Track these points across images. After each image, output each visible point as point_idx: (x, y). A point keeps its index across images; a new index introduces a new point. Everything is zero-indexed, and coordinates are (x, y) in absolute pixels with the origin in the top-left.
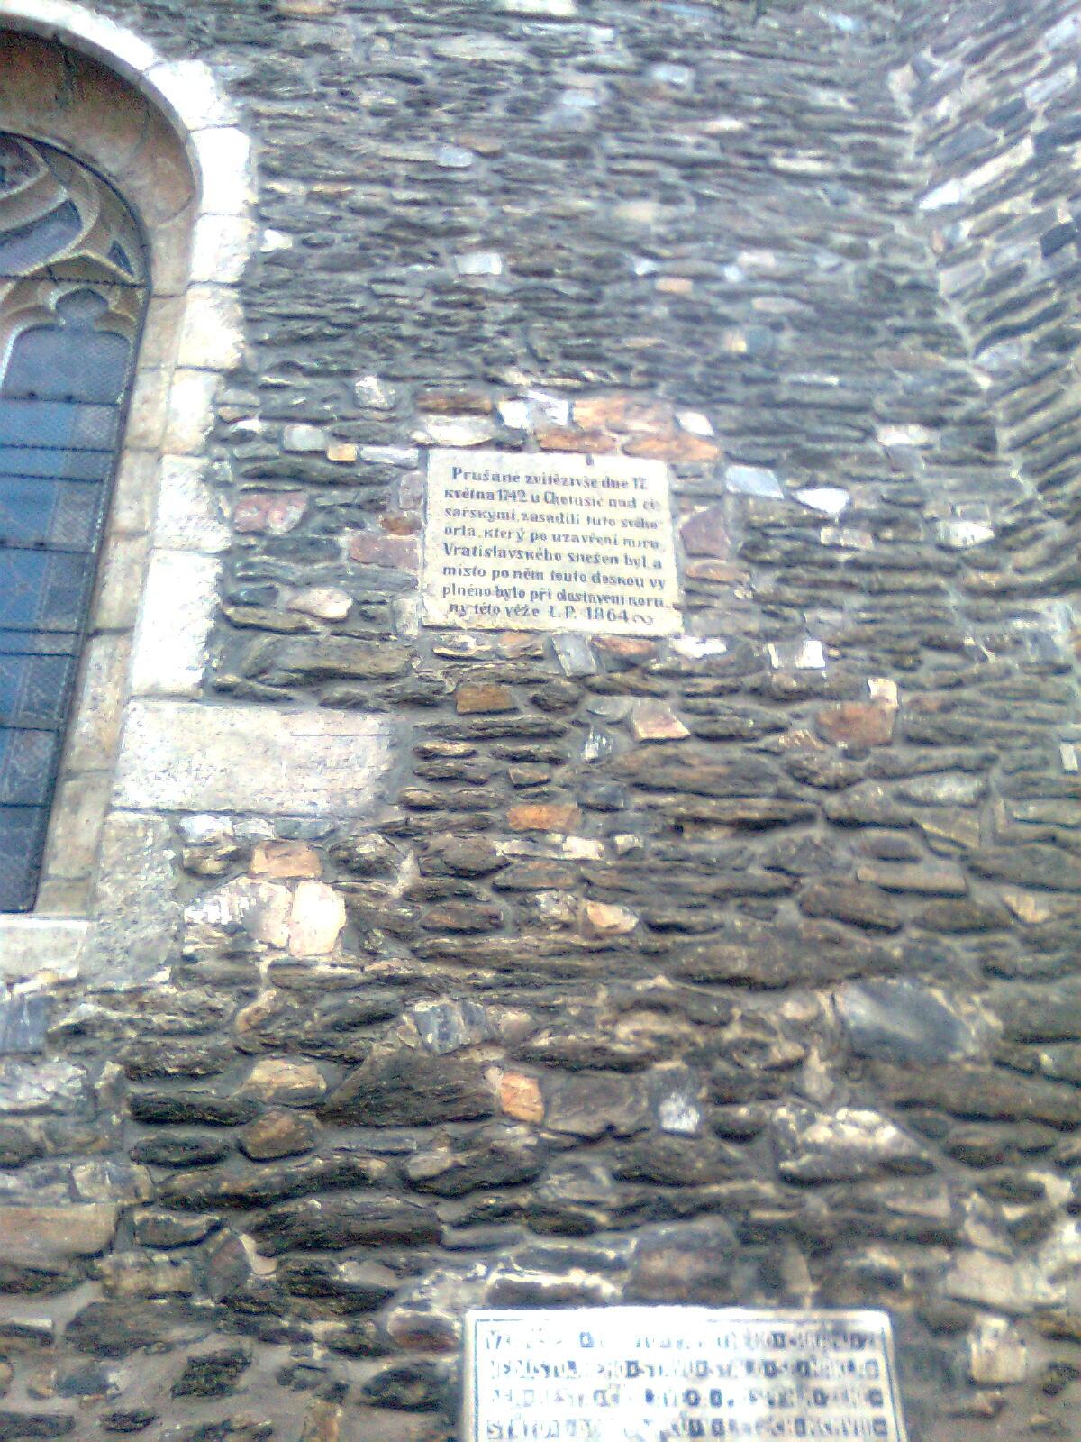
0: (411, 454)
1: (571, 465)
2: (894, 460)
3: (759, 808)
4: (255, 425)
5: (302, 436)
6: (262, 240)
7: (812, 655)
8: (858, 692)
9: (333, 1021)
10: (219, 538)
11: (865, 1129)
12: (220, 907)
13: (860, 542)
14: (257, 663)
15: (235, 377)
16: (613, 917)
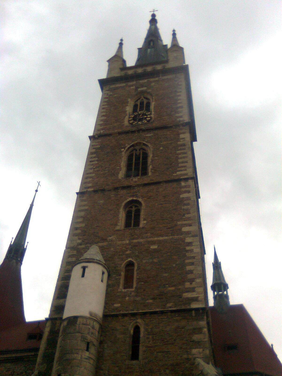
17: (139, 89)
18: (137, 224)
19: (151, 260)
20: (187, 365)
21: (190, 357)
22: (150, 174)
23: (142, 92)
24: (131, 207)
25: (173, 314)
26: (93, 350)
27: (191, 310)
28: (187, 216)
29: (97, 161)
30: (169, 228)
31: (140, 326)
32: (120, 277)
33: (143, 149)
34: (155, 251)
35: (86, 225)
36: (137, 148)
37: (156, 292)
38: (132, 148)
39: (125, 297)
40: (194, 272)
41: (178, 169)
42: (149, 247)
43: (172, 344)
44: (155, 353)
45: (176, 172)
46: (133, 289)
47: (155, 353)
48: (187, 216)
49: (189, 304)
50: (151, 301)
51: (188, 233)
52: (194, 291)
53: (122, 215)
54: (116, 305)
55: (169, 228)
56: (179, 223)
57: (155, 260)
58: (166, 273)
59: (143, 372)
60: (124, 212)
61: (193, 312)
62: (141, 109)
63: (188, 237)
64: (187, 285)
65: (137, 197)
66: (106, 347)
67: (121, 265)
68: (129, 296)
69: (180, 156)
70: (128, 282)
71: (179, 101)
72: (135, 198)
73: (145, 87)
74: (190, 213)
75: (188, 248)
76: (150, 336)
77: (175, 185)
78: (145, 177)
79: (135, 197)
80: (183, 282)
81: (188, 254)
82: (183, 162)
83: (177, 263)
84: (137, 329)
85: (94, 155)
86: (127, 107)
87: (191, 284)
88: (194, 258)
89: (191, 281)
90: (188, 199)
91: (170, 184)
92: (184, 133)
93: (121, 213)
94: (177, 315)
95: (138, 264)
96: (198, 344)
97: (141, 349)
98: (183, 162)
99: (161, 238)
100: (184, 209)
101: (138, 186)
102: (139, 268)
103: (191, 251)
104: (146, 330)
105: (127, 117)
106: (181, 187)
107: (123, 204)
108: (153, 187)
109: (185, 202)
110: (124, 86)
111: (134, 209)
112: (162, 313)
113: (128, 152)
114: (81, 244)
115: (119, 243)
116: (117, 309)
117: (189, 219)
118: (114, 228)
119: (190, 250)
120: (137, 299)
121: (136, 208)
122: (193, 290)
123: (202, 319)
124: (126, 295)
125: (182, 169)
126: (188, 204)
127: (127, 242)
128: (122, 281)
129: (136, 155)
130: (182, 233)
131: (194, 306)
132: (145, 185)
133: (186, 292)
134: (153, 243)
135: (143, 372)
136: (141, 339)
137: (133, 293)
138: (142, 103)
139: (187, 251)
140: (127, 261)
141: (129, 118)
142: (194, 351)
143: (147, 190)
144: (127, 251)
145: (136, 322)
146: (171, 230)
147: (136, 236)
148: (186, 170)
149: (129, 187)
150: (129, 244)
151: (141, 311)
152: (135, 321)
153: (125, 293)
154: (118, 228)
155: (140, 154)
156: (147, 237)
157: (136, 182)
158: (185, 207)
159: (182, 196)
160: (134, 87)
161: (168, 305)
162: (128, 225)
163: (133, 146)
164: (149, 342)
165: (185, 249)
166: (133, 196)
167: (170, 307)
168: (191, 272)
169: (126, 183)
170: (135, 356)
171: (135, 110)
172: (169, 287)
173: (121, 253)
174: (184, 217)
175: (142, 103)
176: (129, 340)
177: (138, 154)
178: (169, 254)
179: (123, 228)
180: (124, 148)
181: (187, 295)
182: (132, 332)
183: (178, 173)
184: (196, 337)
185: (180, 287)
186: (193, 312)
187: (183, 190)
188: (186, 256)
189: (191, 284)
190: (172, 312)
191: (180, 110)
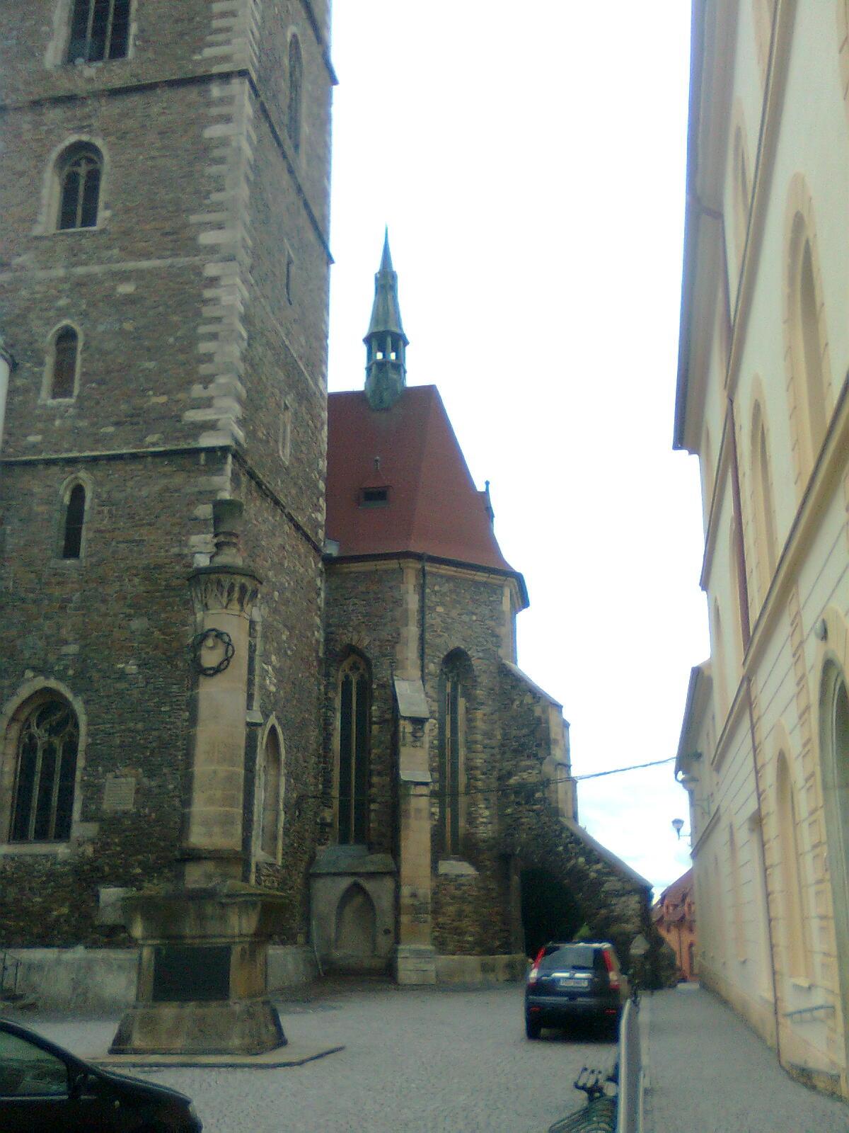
0: (104, 780)
1: (123, 780)
2: (165, 774)
3: (136, 832)
4: (86, 778)
5: (92, 779)
6: (87, 740)
7: (147, 811)
8: (151, 816)
9: (91, 862)
10: (82, 797)
11: (138, 871)
12: (81, 850)
13: (156, 791)
14: (86, 818)
15: (85, 769)
16: (118, 849)
18: (89, 219)
19: (117, 327)
20: (177, 567)
21: (186, 551)
22: (131, 52)
24: (77, 164)
25: (158, 460)
27: (198, 451)
28: (216, 197)
30: (167, 234)
31: (83, 484)
32: (42, 368)
34: (130, 300)
37: (123, 407)
39: (52, 419)
40: (217, 359)
41: (209, 38)
42: (114, 288)
43: (150, 524)
44: (114, 544)
45: (199, 50)
46: (72, 401)
47: (114, 544)
48: (216, 197)
49: (196, 437)
50: (111, 429)
51: (213, 249)
52: (210, 406)
53: (51, 190)
54: (32, 439)
55: (167, 234)
56: (193, 219)
57: (128, 326)
58: (151, 360)
59: (86, 582)
60: (57, 180)
61: (203, 456)
63: (211, 261)
64: (197, 390)
65: (90, 132)
66: (8, 532)
67: (44, 336)
68: (62, 417)
70: (62, 384)
72: (85, 138)
74: (220, 190)
75: (208, 294)
76: (106, 509)
77: (192, 94)
78: (115, 64)
79: (88, 132)
80: (187, 384)
81: (208, 311)
82: (224, 15)
83: (179, 334)
84: (78, 493)
87: (205, 388)
88: (218, 320)
89: (207, 380)
90: (224, 142)
91: (182, 92)
93: (48, 183)
94: (166, 463)
95: (86, 335)
97: (85, 535)
98: (224, 15)
99: (145, 264)
100: (210, 177)
101: (97, 95)
102: (87, 346)
103: (215, 301)
104: (98, 496)
106: (209, 104)
107: (54, 155)
108: (136, 100)
109: (216, 153)
111: (83, 170)
112: (134, 457)
115: (41, 275)
116: (34, 446)
117: (219, 207)
118: (30, 229)
119: (211, 300)
120: (81, 424)
121: (91, 167)
122: (207, 403)
123: (220, 471)
124: (55, 416)
125: (220, 37)
126: (221, 161)
128: (47, 379)
131: (207, 441)
132: (115, 93)
133: (193, 408)
134: (124, 277)
135: (86, 582)
136: (85, 514)
137: (71, 410)
139: (206, 302)
140: (59, 326)
142: (194, 539)
143: (118, 111)
144: (58, 298)
145: (76, 478)
146: (171, 241)
147: (84, 257)
148: (228, 42)
149: (69, 100)
150: (64, 280)
151: (87, 454)
152: (73, 476)
153: (52, 408)
154: (38, 230)
156: (110, 260)
157: (90, 80)
158: (214, 170)
161: (149, 439)
162: (67, 220)
164: (103, 520)
165: (200, 295)
166: (80, 129)
167: (154, 444)
168: (209, 358)
169: (64, 86)
170: (71, 549)
172: (155, 395)
173: (46, 305)
174: (207, 202)
176: (59, 517)
178: (161, 309)
179: (53, 229)
181: (193, 416)
182: (67, 500)
183: (208, 52)
186: (203, 456)
187: (214, 111)
188: (198, 313)
189: (205, 388)
190: (155, 455)
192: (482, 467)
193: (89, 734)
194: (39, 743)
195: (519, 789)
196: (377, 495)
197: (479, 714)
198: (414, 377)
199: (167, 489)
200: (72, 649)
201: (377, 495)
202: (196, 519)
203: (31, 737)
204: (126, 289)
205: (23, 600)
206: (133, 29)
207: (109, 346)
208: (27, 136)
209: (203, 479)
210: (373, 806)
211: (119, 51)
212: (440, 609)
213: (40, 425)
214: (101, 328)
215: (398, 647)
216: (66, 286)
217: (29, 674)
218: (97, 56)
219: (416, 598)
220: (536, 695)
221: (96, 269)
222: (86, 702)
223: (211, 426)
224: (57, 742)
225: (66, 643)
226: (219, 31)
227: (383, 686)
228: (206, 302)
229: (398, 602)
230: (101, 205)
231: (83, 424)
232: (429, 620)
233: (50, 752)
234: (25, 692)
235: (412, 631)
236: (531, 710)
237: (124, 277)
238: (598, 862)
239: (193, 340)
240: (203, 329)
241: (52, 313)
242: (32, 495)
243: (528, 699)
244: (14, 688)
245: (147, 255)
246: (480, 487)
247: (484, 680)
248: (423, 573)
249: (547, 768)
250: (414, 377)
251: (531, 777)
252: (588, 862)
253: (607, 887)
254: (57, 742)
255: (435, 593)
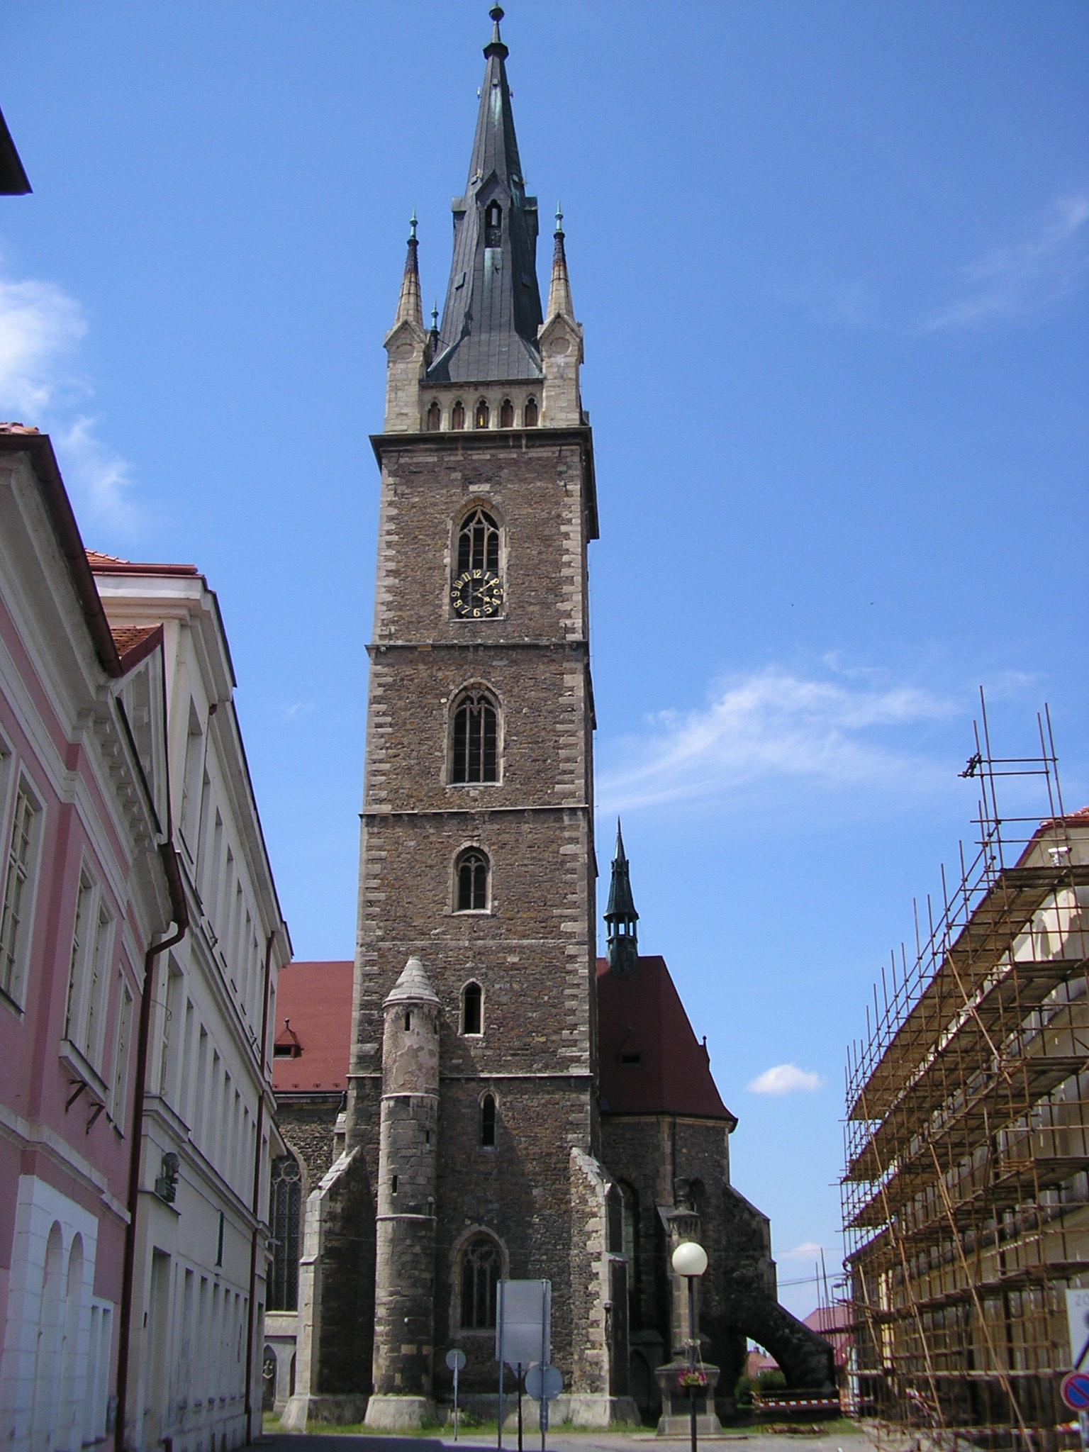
17: (472, 488)
18: (481, 904)
23: (479, 500)
24: (468, 860)
26: (433, 1139)
29: (391, 725)
33: (489, 702)
35: (389, 898)
36: (474, 694)
38: (464, 693)
41: (559, 777)
42: (505, 958)
46: (481, 1035)
51: (571, 935)
53: (452, 881)
56: (556, 912)
62: (478, 565)
69: (562, 740)
71: (565, 558)
72: (475, 844)
73: (488, 480)
75: (569, 967)
80: (558, 1031)
85: (383, 707)
86: (446, 552)
88: (578, 985)
89: (573, 1027)
90: (574, 857)
92: (573, 672)
96: (575, 1126)
98: (567, 760)
99: (526, 942)
103: (575, 972)
105: (447, 588)
106: (563, 829)
107: (454, 855)
110: (434, 464)
111: (473, 865)
113: (455, 705)
114: (382, 939)
117: (574, 905)
122: (574, 1043)
125: (566, 777)
126: (573, 871)
127: (467, 944)
129: (471, 712)
130: (561, 935)
134: (512, 950)
138: (479, 533)
139: (568, 972)
141: (453, 589)
142: (570, 1136)
154: (447, 910)
155: (479, 712)
159: (562, 850)
160: (458, 475)
163: (465, 688)
167: (540, 1071)
168: (572, 1012)
170: (488, 1139)
171: (462, 566)
175: (479, 533)
176: (479, 1117)
177: (475, 713)
180: (446, 695)
184: (572, 1117)
185: (554, 1038)
187: (567, 834)
191: (566, 589)
192: (700, 1028)
193: (511, 1262)
194: (475, 1266)
195: (742, 1279)
196: (634, 1059)
197: (711, 1227)
198: (643, 950)
199: (548, 1102)
200: (496, 1206)
201: (634, 1059)
202: (571, 1123)
203: (469, 1261)
204: (512, 959)
205: (460, 1172)
206: (502, 762)
207: (504, 999)
208: (433, 839)
209: (574, 1095)
210: (643, 1297)
211: (491, 775)
212: (684, 1151)
213: (460, 1052)
214: (497, 986)
215: (658, 1181)
216: (470, 953)
217: (468, 1222)
218: (474, 777)
219: (669, 1143)
220: (754, 1213)
221: (491, 943)
222: (507, 1242)
223: (577, 1060)
224: (487, 1266)
225: (491, 1202)
226: (565, 772)
227: (647, 1210)
228: (568, 972)
229: (657, 1147)
230: (490, 896)
231: (489, 1053)
232: (678, 1160)
233: (482, 1272)
234: (466, 1234)
235: (669, 1168)
236: (749, 1225)
237: (512, 950)
238: (798, 1332)
239: (561, 998)
240: (567, 992)
241: (462, 973)
242: (459, 1101)
243: (746, 1216)
244: (459, 1230)
245: (524, 937)
246: (701, 1042)
247: (713, 1201)
248: (673, 1126)
249: (762, 1265)
250: (643, 950)
251: (750, 1272)
252: (792, 1332)
253: (806, 1349)
254: (487, 1266)
255: (681, 1138)
